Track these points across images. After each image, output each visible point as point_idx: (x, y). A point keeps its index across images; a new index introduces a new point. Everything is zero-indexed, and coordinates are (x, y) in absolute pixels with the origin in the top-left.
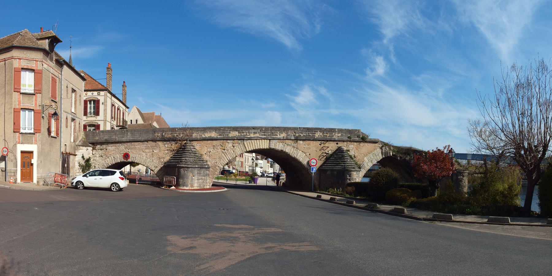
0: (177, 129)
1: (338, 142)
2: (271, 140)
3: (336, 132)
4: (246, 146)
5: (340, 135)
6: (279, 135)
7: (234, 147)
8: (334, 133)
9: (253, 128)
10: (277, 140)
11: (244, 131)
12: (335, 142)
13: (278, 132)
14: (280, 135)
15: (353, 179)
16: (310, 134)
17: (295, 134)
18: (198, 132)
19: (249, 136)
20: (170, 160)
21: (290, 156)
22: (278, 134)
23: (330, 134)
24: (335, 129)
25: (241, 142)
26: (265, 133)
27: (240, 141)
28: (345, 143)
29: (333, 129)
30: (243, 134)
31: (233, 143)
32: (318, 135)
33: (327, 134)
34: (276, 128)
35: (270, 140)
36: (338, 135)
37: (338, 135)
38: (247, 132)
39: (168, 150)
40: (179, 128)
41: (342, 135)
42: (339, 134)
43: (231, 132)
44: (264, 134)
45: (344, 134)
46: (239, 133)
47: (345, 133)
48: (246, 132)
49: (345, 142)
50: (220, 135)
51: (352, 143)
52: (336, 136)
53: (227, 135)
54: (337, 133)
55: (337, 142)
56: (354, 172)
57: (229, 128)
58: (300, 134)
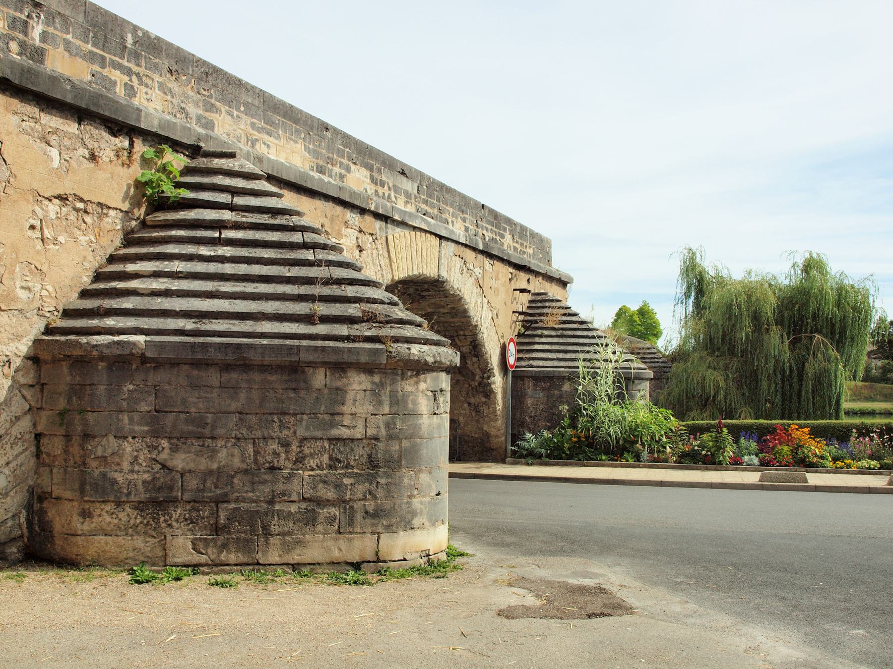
0: (130, 40)
2: (444, 243)
4: (393, 256)
6: (450, 224)
7: (360, 251)
9: (403, 173)
10: (453, 244)
11: (384, 178)
12: (527, 276)
13: (451, 210)
14: (453, 222)
16: (498, 238)
17: (477, 230)
18: (238, 110)
19: (396, 204)
20: (85, 294)
21: (469, 317)
22: (450, 220)
23: (522, 244)
25: (380, 229)
26: (426, 202)
27: (378, 224)
30: (381, 191)
31: (361, 231)
32: (508, 244)
33: (517, 242)
34: (449, 190)
35: (441, 237)
38: (391, 185)
39: (63, 198)
40: (146, 33)
43: (353, 167)
44: (423, 206)
46: (373, 181)
48: (388, 184)
50: (321, 170)
53: (342, 177)
57: (348, 140)
58: (485, 232)
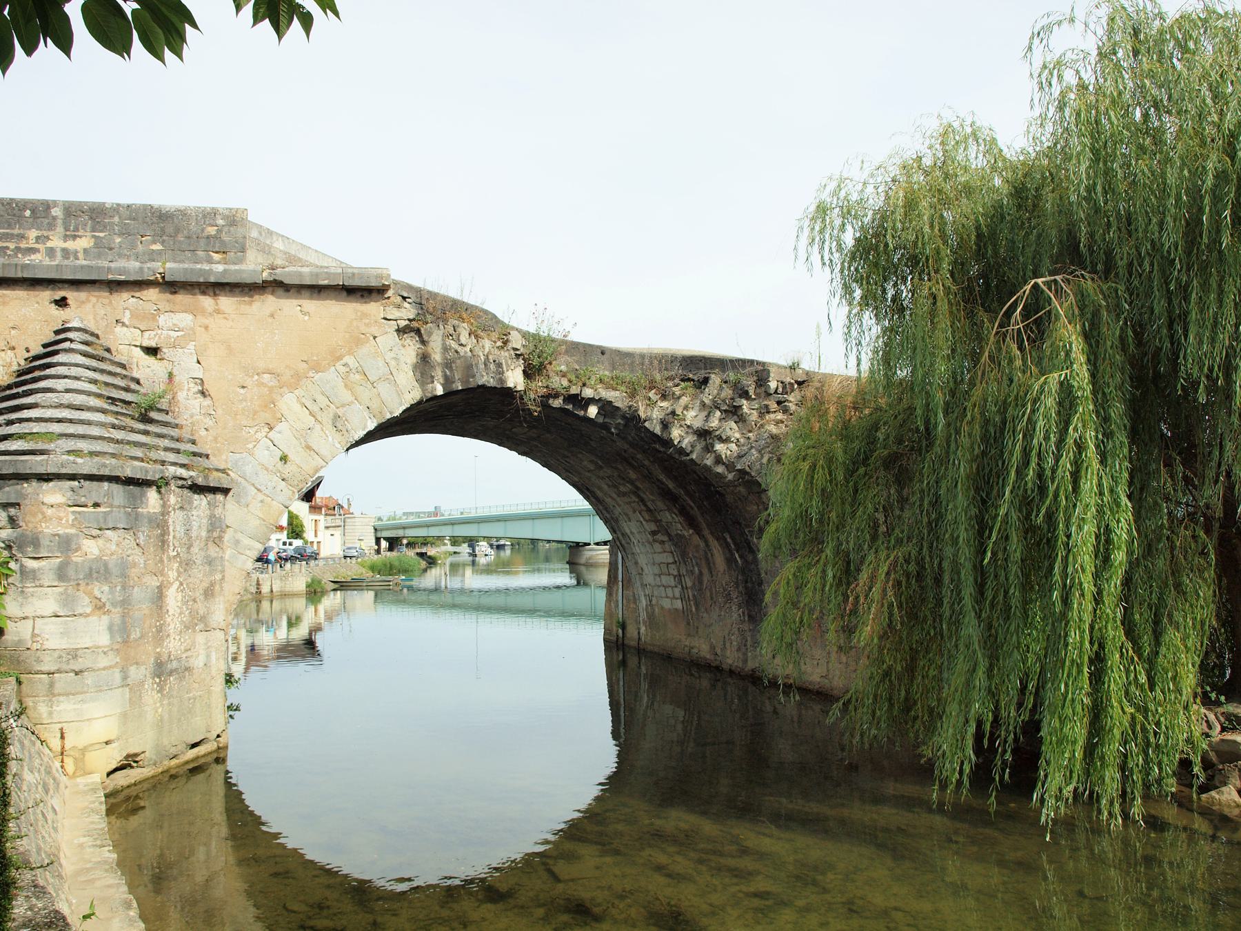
1: (71, 295)
3: (51, 226)
5: (84, 243)
8: (33, 234)
12: (47, 295)
15: (36, 543)
24: (47, 206)
28: (125, 301)
29: (23, 205)
36: (70, 245)
37: (70, 245)
41: (101, 247)
42: (75, 237)
45: (118, 240)
47: (121, 234)
49: (125, 295)
51: (182, 298)
52: (51, 252)
54: (60, 229)
55: (59, 295)
56: (45, 486)
